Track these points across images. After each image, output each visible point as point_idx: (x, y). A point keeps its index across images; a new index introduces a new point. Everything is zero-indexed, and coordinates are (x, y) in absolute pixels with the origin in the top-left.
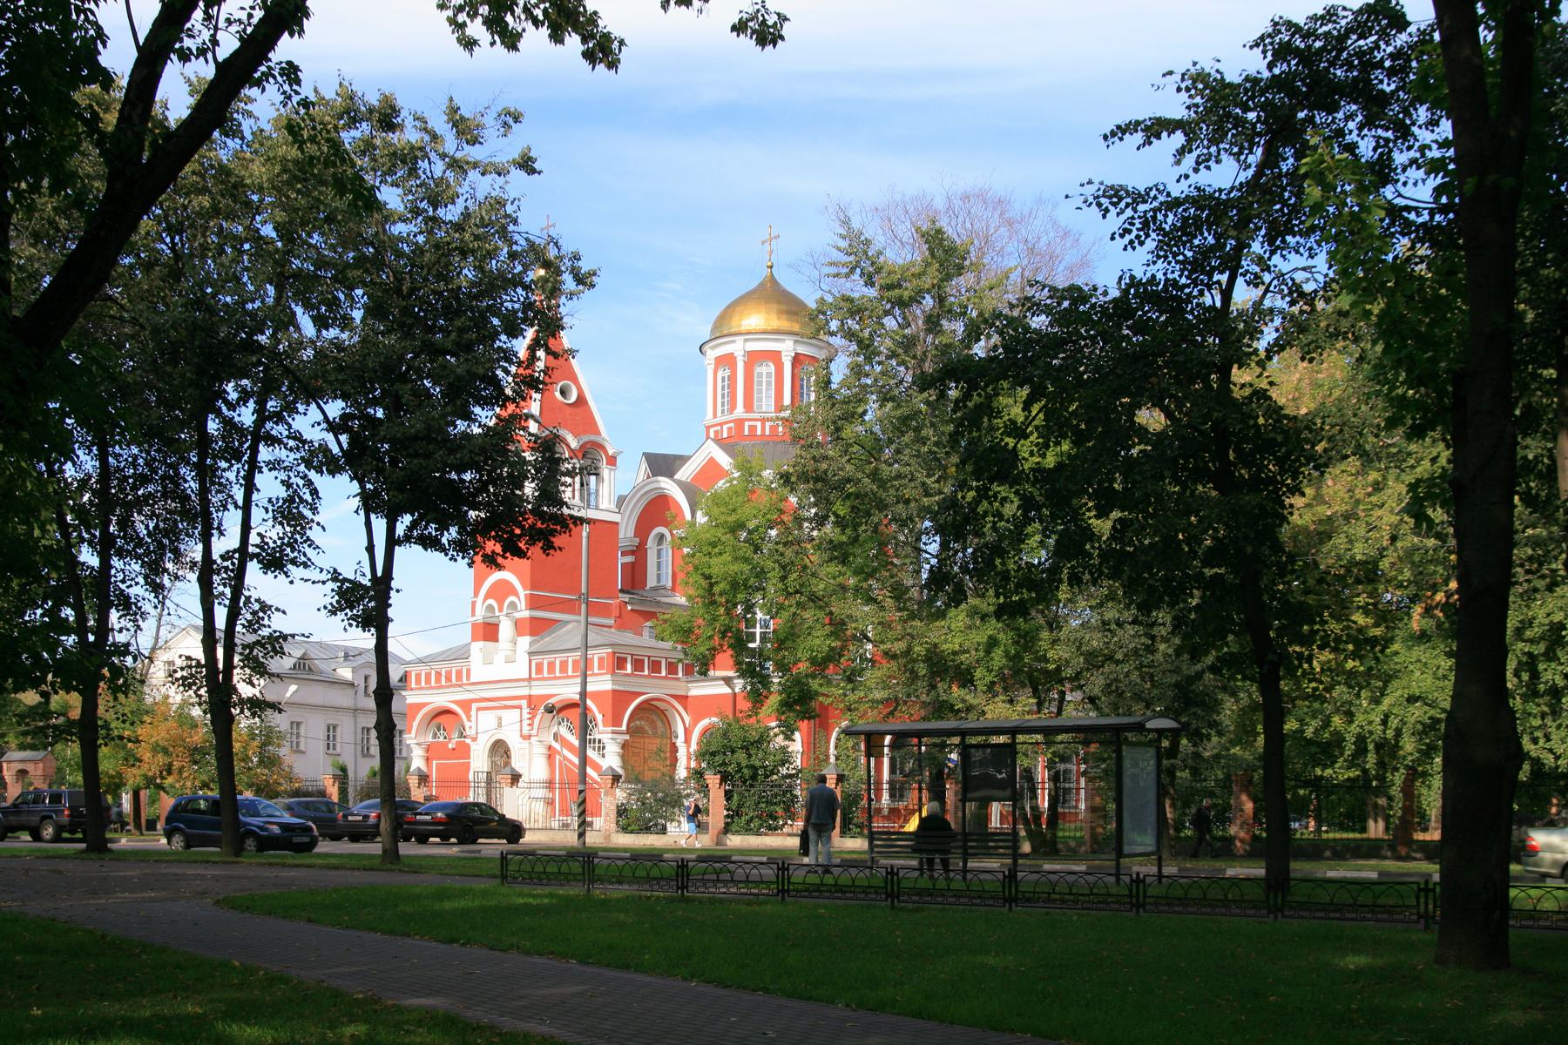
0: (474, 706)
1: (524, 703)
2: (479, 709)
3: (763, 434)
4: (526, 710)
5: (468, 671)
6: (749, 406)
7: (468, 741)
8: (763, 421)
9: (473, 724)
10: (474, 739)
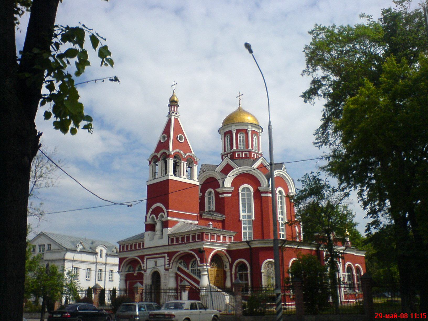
0: (145, 258)
1: (166, 255)
2: (147, 259)
3: (242, 157)
4: (167, 258)
5: (143, 244)
7: (143, 272)
8: (242, 152)
9: (145, 265)
10: (145, 271)
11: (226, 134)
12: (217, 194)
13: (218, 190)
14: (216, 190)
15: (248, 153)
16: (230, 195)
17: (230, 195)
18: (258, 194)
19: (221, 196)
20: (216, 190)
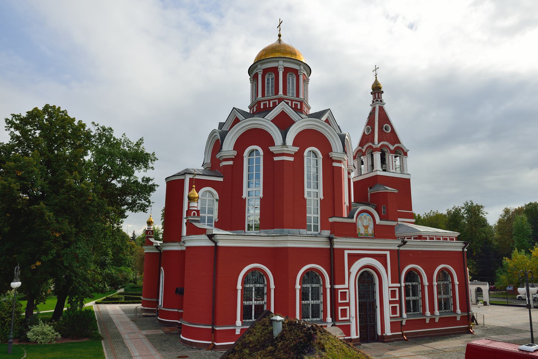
6: (285, 92)
8: (292, 101)
11: (266, 71)
12: (269, 156)
13: (272, 149)
14: (270, 148)
15: (299, 104)
16: (292, 159)
17: (292, 159)
18: (328, 161)
19: (276, 159)
20: (270, 148)
